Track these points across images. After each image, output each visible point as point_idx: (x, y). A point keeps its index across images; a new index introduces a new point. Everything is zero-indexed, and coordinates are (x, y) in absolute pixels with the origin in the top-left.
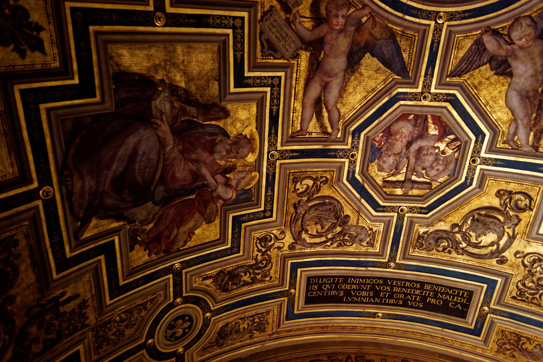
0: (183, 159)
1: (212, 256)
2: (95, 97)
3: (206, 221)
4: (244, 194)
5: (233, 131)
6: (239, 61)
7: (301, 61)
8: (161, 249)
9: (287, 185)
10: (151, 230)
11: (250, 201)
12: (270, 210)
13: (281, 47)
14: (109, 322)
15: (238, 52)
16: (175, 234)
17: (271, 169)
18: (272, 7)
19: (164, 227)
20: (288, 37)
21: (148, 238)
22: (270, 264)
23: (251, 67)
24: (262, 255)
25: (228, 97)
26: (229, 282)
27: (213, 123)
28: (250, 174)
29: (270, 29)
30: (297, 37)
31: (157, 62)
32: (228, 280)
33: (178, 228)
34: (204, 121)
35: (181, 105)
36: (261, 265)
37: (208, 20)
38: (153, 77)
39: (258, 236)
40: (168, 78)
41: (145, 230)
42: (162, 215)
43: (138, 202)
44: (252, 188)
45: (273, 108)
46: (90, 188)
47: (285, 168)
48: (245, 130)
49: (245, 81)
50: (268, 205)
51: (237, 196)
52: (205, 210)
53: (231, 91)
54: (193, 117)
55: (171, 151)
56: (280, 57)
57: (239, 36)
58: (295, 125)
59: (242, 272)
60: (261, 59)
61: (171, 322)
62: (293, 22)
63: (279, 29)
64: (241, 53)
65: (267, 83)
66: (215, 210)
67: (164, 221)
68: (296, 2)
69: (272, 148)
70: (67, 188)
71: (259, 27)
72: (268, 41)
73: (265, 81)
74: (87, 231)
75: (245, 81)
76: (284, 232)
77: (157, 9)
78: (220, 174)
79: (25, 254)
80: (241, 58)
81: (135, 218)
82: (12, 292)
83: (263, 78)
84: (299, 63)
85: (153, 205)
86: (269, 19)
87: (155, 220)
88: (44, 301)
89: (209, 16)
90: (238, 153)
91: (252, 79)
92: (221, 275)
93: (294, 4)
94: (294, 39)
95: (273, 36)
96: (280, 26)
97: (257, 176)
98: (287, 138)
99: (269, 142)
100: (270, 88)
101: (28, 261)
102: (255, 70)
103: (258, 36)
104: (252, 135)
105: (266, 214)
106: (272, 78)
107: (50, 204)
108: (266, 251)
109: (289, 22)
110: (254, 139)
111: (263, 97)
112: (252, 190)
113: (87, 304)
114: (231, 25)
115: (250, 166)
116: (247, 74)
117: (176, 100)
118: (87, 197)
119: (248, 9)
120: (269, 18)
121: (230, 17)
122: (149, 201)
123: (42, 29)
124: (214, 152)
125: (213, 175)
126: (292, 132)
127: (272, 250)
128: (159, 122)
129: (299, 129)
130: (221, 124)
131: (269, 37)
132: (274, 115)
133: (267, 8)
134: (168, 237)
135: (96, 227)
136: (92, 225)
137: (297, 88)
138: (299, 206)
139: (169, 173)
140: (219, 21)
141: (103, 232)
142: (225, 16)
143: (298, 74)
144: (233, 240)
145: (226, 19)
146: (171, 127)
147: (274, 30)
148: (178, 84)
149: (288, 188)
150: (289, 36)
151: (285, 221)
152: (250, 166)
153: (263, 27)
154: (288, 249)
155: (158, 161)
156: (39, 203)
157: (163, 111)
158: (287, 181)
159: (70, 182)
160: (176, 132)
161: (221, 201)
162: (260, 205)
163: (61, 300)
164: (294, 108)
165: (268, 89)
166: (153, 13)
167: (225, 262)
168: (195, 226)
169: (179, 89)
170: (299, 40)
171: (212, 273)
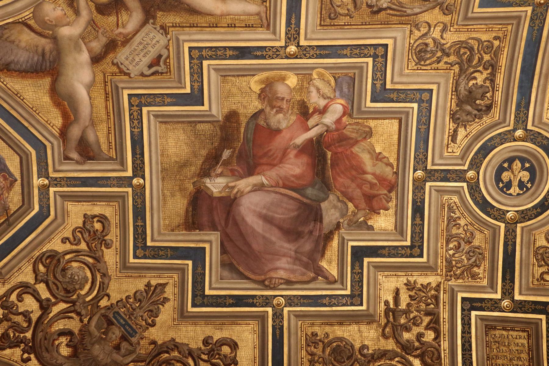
0: (280, 165)
1: (422, 130)
2: (204, 248)
3: (368, 137)
4: (342, 88)
5: (255, 105)
6: (174, 100)
7: (169, 23)
8: (385, 194)
9: (339, 27)
10: (356, 207)
11: (354, 79)
12: (375, 49)
13: (154, 49)
14: (449, 262)
15: (164, 101)
16: (372, 176)
17: (312, 53)
18: (113, 64)
19: (359, 190)
20: (143, 42)
21: (364, 209)
22: (470, 41)
23: (180, 85)
24: (448, 55)
25: (214, 112)
26: (477, 104)
27: (242, 130)
28: (315, 81)
29: (137, 64)
30: (142, 30)
31: (177, 188)
32: (471, 106)
33: (365, 173)
34: (239, 141)
35: (220, 165)
36: (466, 56)
37: (136, 133)
38: (190, 193)
39: (414, 64)
40: (192, 178)
41: (353, 212)
42: (342, 192)
43: (318, 217)
44: (334, 77)
45: (228, 55)
46: (288, 263)
47: (313, 32)
48: (254, 90)
49: (196, 93)
50: (366, 51)
51: (342, 96)
52: (352, 139)
53: (208, 109)
54: (233, 152)
55: (268, 179)
56: (166, 51)
57: (149, 100)
58: (252, 22)
59: (468, 84)
60: (170, 74)
61: (498, 187)
62: (125, 36)
63: (135, 54)
64: (166, 98)
65: (197, 65)
66: (354, 127)
67: (350, 190)
68: (103, 35)
69: (281, 53)
70: (281, 284)
71: (136, 77)
72: (150, 66)
73: (196, 67)
74: (331, 272)
75: (196, 93)
76: (418, 24)
77: (130, 185)
78: (307, 120)
79: (328, 329)
80: (171, 97)
81: (335, 222)
82: (357, 345)
83: (192, 70)
84: (171, 25)
85: (326, 202)
86: (126, 66)
87: (345, 200)
88: (383, 321)
89: (132, 132)
90: (283, 99)
91: (193, 84)
92: (458, 116)
93: (106, 37)
94: (143, 34)
95: (143, 59)
96: (132, 52)
97: (318, 71)
98: (269, 33)
99: (273, 58)
100: (204, 62)
101: (336, 328)
102: (183, 81)
103: (146, 78)
104: (261, 82)
105: (380, 54)
106: (191, 58)
107: (291, 301)
108: (443, 51)
109: (127, 40)
110: (267, 78)
111: (215, 70)
112: (339, 77)
113: (412, 282)
114: (138, 108)
115: (303, 82)
116: (188, 90)
117: (215, 170)
118: (295, 267)
119: (120, 90)
120: (125, 67)
121: (130, 110)
122: (320, 205)
123: (149, 283)
124: (278, 128)
125: (308, 129)
126: (261, 27)
127: (443, 42)
128: (236, 190)
129: (257, 17)
130: (244, 121)
131: (145, 66)
132: (237, 53)
133: (115, 69)
134: (372, 185)
135: (330, 262)
136: (326, 266)
137: (203, 25)
138: (377, 5)
139: (293, 182)
140: (136, 122)
141: (338, 256)
142: (130, 115)
143: (184, 25)
144: (408, 100)
145: (132, 114)
146: (242, 177)
147: (137, 59)
148: (198, 168)
149: (345, 25)
150: (141, 41)
151: (400, 24)
152: (303, 82)
153: (136, 73)
154: (450, 16)
155: (276, 193)
156: (286, 310)
157: (225, 185)
158: (333, 27)
159: (277, 280)
160: (250, 173)
161: (344, 119)
162: (363, 64)
163: (392, 306)
164: (228, 27)
165: (205, 63)
166: (134, 189)
167: (439, 112)
168: (369, 153)
169: (203, 167)
170: (144, 28)
171: (450, 129)
